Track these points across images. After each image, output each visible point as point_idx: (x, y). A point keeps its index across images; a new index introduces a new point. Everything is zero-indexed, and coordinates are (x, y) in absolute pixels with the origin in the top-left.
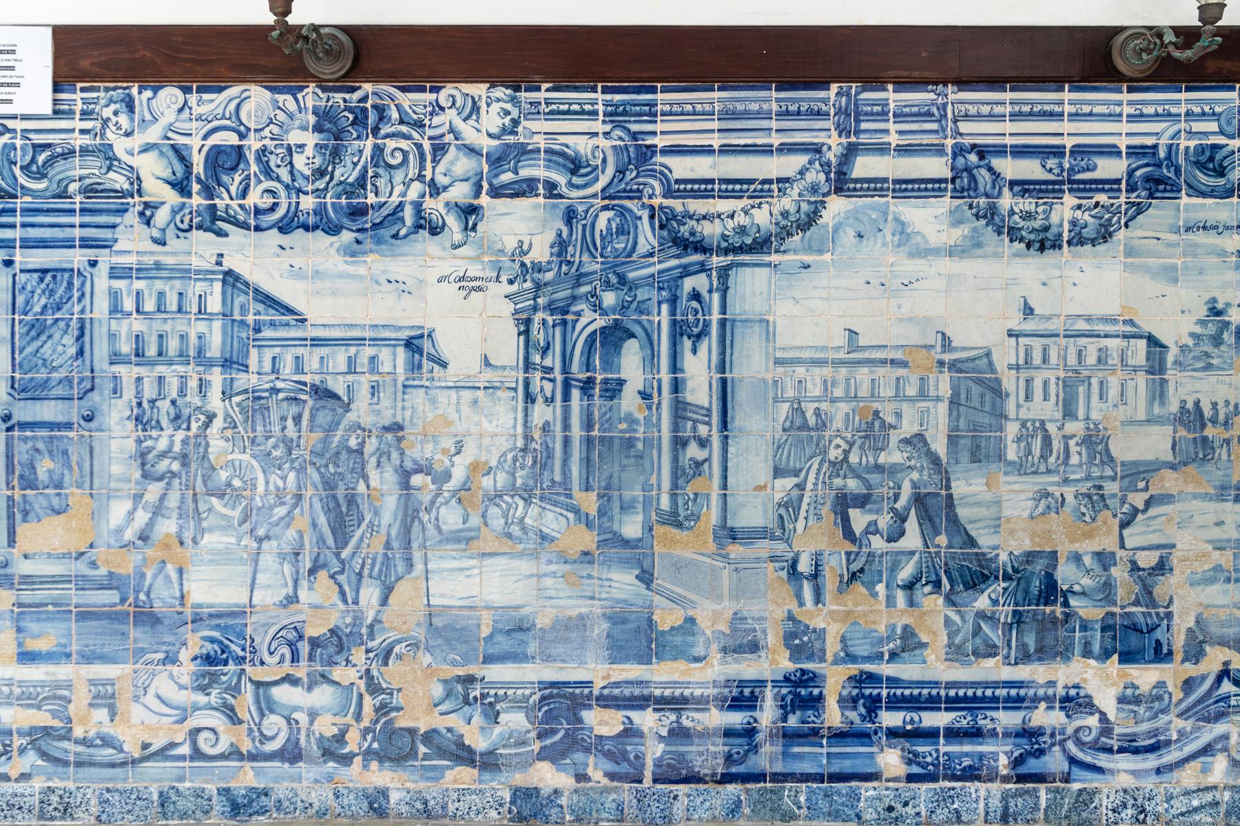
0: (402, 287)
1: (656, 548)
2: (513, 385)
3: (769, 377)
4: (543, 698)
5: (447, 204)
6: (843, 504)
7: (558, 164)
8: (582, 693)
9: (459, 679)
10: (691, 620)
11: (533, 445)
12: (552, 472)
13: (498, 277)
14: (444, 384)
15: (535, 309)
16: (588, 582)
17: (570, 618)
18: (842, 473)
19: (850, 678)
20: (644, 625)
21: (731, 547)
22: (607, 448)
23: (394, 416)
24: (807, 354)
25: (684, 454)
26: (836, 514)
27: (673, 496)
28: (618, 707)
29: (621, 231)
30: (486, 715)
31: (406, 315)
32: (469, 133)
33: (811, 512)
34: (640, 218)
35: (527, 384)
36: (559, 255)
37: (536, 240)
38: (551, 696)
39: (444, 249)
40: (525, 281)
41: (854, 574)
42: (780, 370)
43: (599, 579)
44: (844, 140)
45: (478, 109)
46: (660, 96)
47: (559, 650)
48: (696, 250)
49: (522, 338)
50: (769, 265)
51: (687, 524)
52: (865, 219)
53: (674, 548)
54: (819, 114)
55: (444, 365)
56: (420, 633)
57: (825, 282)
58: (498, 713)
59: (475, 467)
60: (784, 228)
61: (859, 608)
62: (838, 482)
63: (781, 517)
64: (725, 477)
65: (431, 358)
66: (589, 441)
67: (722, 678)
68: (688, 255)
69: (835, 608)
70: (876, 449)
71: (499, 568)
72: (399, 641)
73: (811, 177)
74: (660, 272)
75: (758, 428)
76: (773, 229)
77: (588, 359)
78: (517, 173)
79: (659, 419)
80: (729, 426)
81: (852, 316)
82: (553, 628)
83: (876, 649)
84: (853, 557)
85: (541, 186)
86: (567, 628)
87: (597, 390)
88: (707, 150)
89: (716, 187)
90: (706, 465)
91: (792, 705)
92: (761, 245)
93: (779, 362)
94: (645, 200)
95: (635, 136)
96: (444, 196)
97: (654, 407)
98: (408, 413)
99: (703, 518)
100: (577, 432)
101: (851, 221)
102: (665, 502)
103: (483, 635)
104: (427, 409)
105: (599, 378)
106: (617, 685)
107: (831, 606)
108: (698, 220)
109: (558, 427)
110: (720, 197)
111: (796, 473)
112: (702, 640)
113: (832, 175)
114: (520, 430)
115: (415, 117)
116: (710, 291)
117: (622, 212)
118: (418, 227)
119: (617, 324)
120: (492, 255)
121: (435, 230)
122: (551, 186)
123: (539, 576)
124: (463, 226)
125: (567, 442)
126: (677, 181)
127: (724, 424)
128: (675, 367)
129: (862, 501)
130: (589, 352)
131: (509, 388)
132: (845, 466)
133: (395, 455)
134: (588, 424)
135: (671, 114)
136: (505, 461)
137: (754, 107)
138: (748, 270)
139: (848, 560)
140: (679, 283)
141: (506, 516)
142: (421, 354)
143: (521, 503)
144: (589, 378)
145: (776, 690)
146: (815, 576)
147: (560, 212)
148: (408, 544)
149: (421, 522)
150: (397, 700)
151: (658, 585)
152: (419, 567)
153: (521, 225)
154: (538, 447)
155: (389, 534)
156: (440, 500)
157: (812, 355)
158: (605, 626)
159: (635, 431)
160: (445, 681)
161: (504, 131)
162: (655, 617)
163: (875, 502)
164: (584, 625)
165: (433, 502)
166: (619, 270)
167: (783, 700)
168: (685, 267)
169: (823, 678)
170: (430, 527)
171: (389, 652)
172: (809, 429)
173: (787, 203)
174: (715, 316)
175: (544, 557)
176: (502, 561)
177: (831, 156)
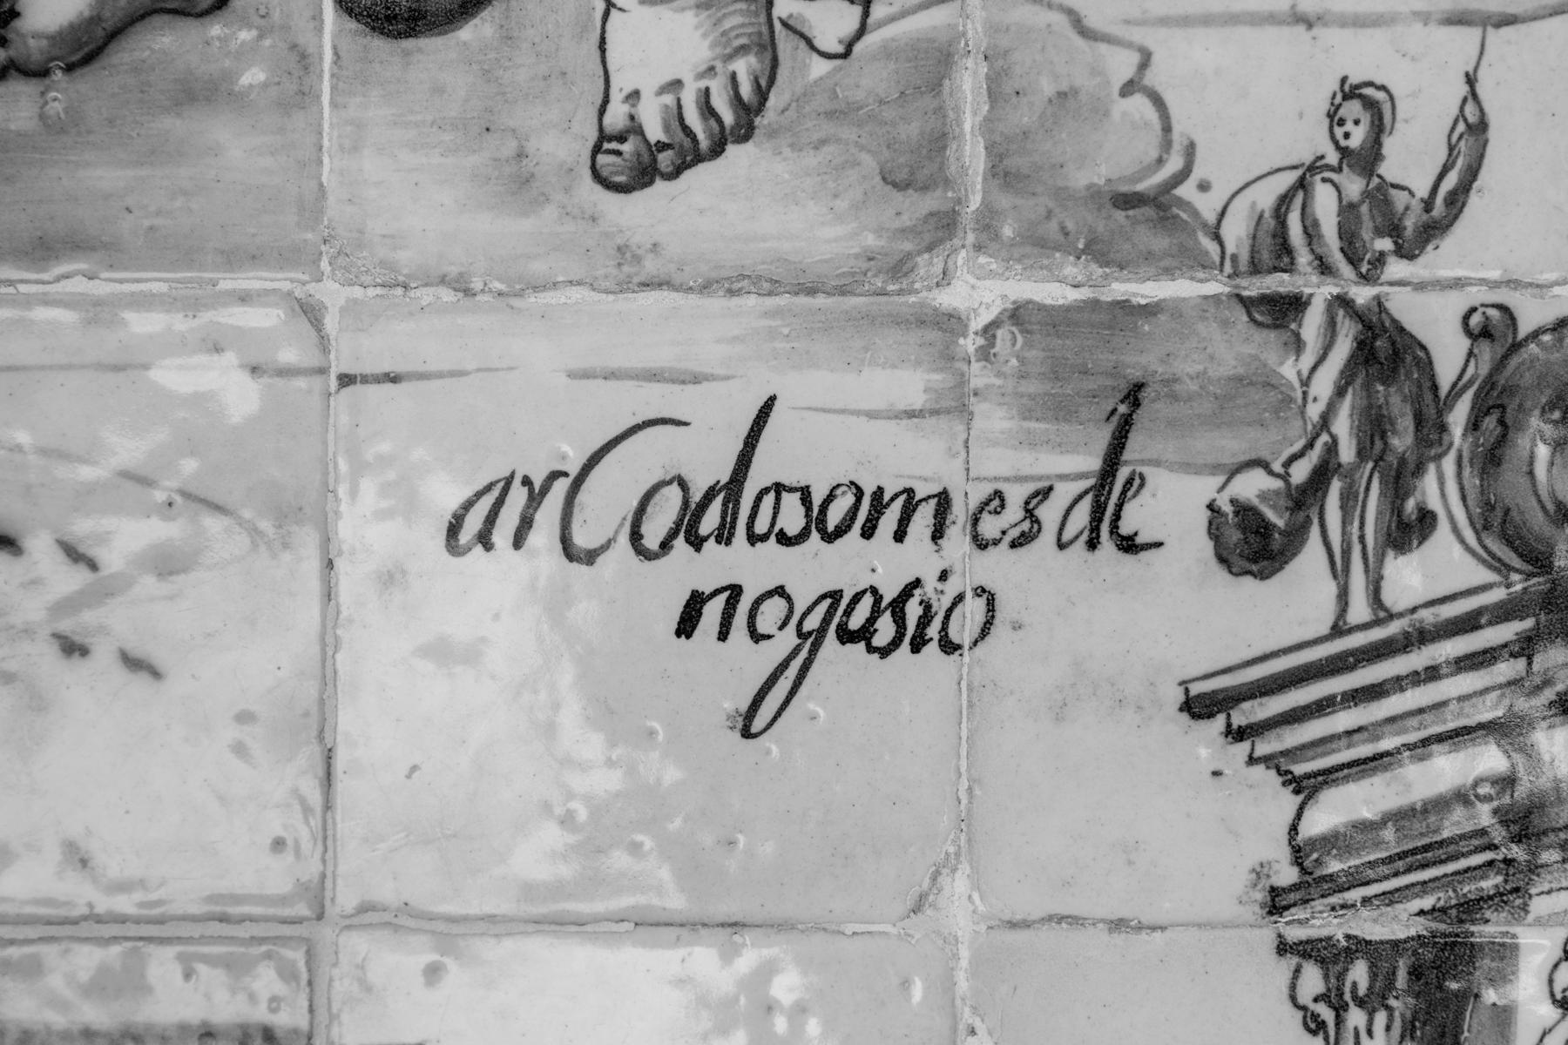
13: (1109, 490)
39: (520, 182)
40: (1409, 530)
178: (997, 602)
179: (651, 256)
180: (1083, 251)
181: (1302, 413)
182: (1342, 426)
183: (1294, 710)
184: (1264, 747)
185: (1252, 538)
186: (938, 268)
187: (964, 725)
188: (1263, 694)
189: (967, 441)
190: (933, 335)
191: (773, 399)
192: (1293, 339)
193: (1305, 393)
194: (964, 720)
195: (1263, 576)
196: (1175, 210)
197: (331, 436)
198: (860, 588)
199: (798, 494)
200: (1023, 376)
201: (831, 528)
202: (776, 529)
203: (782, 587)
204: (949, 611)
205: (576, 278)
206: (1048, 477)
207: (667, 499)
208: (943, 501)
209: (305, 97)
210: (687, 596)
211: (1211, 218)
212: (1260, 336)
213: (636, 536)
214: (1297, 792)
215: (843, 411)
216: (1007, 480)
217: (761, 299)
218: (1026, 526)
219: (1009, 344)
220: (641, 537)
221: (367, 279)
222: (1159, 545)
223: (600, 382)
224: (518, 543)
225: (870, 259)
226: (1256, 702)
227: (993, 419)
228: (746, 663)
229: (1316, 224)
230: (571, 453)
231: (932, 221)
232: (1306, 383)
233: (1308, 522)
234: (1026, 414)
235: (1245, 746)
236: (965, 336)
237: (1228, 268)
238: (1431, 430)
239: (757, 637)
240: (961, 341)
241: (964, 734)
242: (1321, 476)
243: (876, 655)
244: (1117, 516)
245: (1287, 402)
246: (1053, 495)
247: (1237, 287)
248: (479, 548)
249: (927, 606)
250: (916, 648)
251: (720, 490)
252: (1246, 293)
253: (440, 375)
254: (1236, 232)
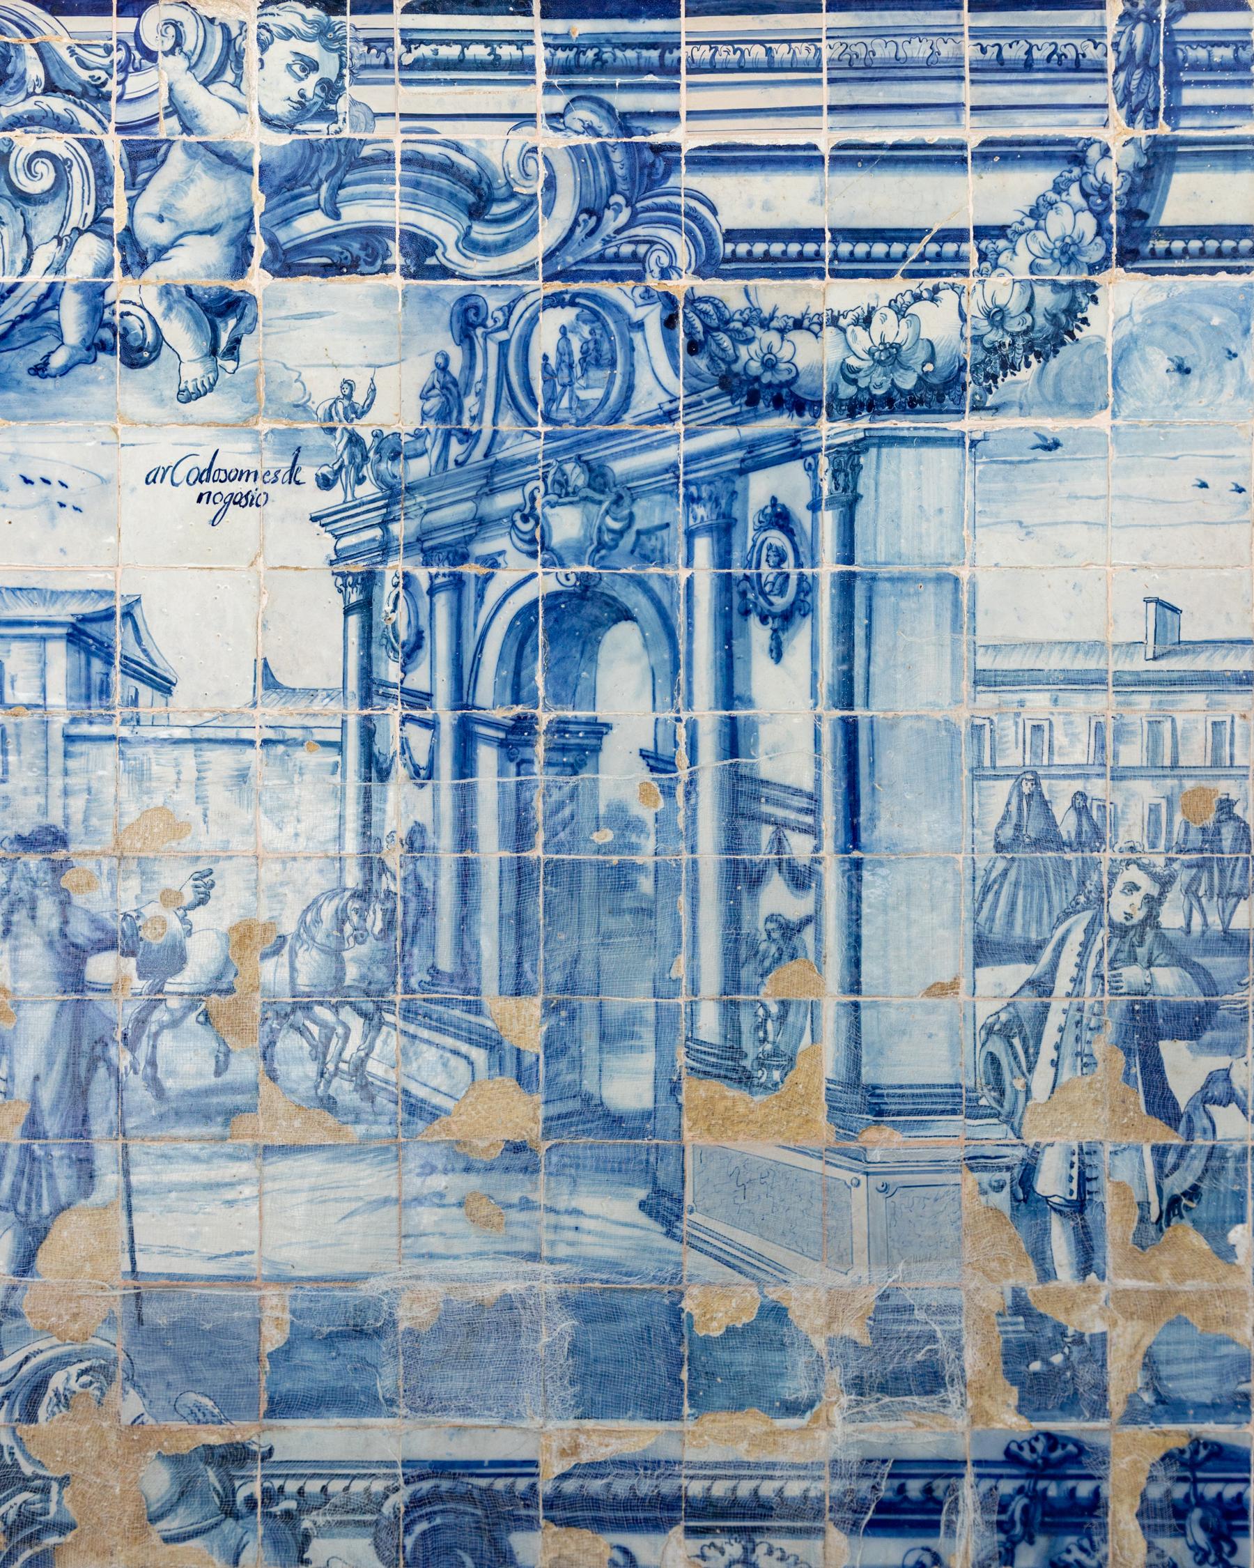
0: (58, 493)
1: (687, 1135)
2: (335, 736)
3: (961, 717)
4: (416, 1502)
5: (166, 291)
6: (1146, 1027)
7: (439, 191)
8: (510, 1490)
9: (210, 1454)
10: (776, 1313)
11: (386, 883)
12: (433, 949)
13: (293, 471)
14: (163, 733)
15: (385, 549)
16: (523, 1216)
17: (481, 1306)
18: (1141, 952)
19: (1168, 1458)
20: (661, 1323)
21: (872, 1134)
22: (566, 890)
23: (45, 811)
24: (1054, 662)
25: (755, 905)
26: (1128, 1052)
27: (730, 1009)
28: (600, 1525)
29: (594, 358)
30: (276, 1543)
31: (72, 562)
32: (217, 116)
33: (1069, 1047)
34: (640, 326)
35: (368, 734)
36: (443, 416)
37: (386, 381)
38: (435, 1496)
39: (161, 401)
40: (360, 481)
41: (1175, 1201)
42: (988, 699)
43: (551, 1210)
44: (1141, 133)
45: (239, 56)
46: (685, 25)
47: (454, 1382)
48: (778, 404)
49: (354, 620)
50: (958, 441)
51: (762, 1076)
52: (1194, 327)
53: (730, 1135)
54: (1079, 67)
55: (164, 686)
56: (114, 1342)
57: (1096, 484)
58: (307, 1538)
59: (242, 937)
60: (994, 349)
61: (1189, 1285)
62: (1133, 975)
63: (993, 1060)
64: (856, 963)
65: (133, 670)
66: (521, 875)
67: (854, 1455)
68: (758, 417)
69: (1129, 1283)
70: (1225, 895)
71: (306, 1183)
72: (62, 1362)
73: (1060, 223)
74: (690, 459)
75: (932, 838)
76: (968, 352)
77: (517, 673)
78: (336, 215)
79: (692, 819)
80: (864, 837)
81: (1163, 568)
82: (438, 1331)
83: (1230, 1387)
84: (1171, 1159)
85: (395, 247)
86: (472, 1330)
87: (540, 749)
88: (801, 159)
89: (827, 248)
90: (808, 933)
91: (1026, 1522)
92: (939, 392)
93: (983, 680)
94: (652, 282)
95: (624, 122)
96: (159, 272)
97: (680, 790)
98: (77, 804)
99: (801, 1062)
100: (491, 851)
101: (1159, 332)
102: (709, 1024)
103: (268, 1348)
104: (123, 794)
105: (545, 718)
106: (595, 1469)
107: (1119, 1277)
108: (782, 331)
109: (446, 840)
110: (836, 274)
111: (1030, 953)
112: (802, 1360)
113: (1113, 219)
114: (352, 844)
115: (84, 75)
116: (814, 507)
117: (596, 311)
118: (95, 347)
119: (585, 590)
120: (277, 416)
121: (138, 355)
122: (421, 248)
123: (404, 1203)
124: (206, 346)
125: (467, 875)
126: (730, 235)
127: (852, 834)
128: (730, 692)
129: (1194, 1023)
130: (520, 655)
131: (325, 744)
132: (1150, 935)
133: (47, 907)
134: (519, 831)
135: (713, 68)
136: (318, 921)
137: (918, 50)
138: (907, 453)
139: (1160, 1166)
140: (739, 484)
141: (320, 1054)
142: (109, 661)
143: (357, 1024)
144: (519, 719)
145: (986, 1484)
146: (1079, 1204)
147: (443, 313)
148: (81, 1126)
149: (114, 1071)
150: (59, 1505)
151: (694, 1225)
152: (109, 1180)
153: (349, 344)
154: (397, 887)
155: (34, 1100)
156: (160, 1015)
157: (1066, 663)
158: (567, 1324)
159: (633, 848)
160: (176, 1460)
161: (302, 108)
162: (687, 1305)
163: (1224, 1025)
164: (515, 1324)
165: (141, 1022)
166: (591, 454)
167: (1003, 1508)
168: (752, 446)
169: (1103, 1457)
170: (135, 1082)
171: (38, 1387)
172: (1062, 845)
173: (1001, 288)
174: (827, 568)
175: (415, 1157)
176: (312, 1165)
177: (1110, 173)
182: (345, 457)
209: (113, 382)
227: (267, 454)
228: (212, 509)
238: (365, 458)
242: (341, 467)
254: (320, 413)
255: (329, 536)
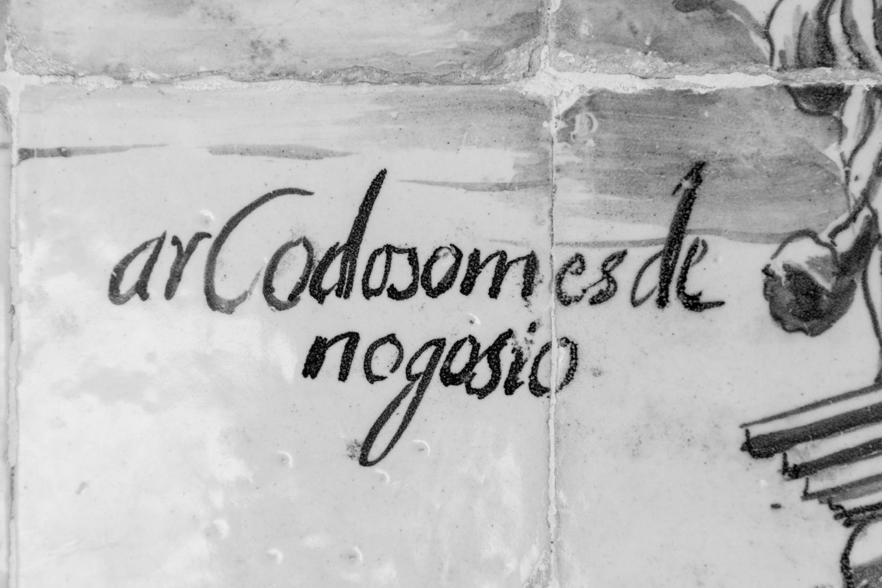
178: (579, 352)
179: (279, 50)
180: (650, 48)
181: (846, 189)
183: (843, 452)
184: (818, 484)
185: (803, 299)
186: (524, 62)
187: (552, 458)
188: (815, 437)
189: (551, 211)
190: (520, 119)
191: (383, 173)
192: (836, 125)
193: (847, 173)
194: (553, 454)
195: (813, 332)
196: (730, 13)
197: (13, 201)
198: (460, 337)
199: (406, 255)
200: (599, 155)
201: (434, 284)
202: (388, 285)
203: (393, 335)
204: (538, 359)
205: (215, 69)
206: (622, 243)
207: (295, 258)
208: (531, 263)
210: (312, 341)
211: (761, 19)
212: (806, 122)
213: (268, 289)
214: (847, 524)
215: (444, 184)
216: (586, 245)
217: (373, 87)
218: (604, 285)
219: (586, 127)
220: (273, 290)
221: (42, 69)
222: (721, 303)
223: (237, 157)
224: (169, 293)
225: (466, 53)
226: (809, 444)
228: (362, 400)
229: (854, 25)
230: (212, 218)
231: (519, 21)
232: (848, 163)
233: (853, 285)
234: (603, 188)
235: (800, 483)
236: (548, 120)
237: (777, 63)
239: (372, 378)
240: (545, 124)
241: (552, 466)
243: (475, 396)
244: (683, 278)
245: (832, 181)
246: (627, 259)
247: (785, 79)
248: (137, 297)
249: (518, 354)
250: (510, 389)
251: (340, 251)
252: (793, 85)
253: (103, 150)
254: (784, 32)
255: (823, 512)
